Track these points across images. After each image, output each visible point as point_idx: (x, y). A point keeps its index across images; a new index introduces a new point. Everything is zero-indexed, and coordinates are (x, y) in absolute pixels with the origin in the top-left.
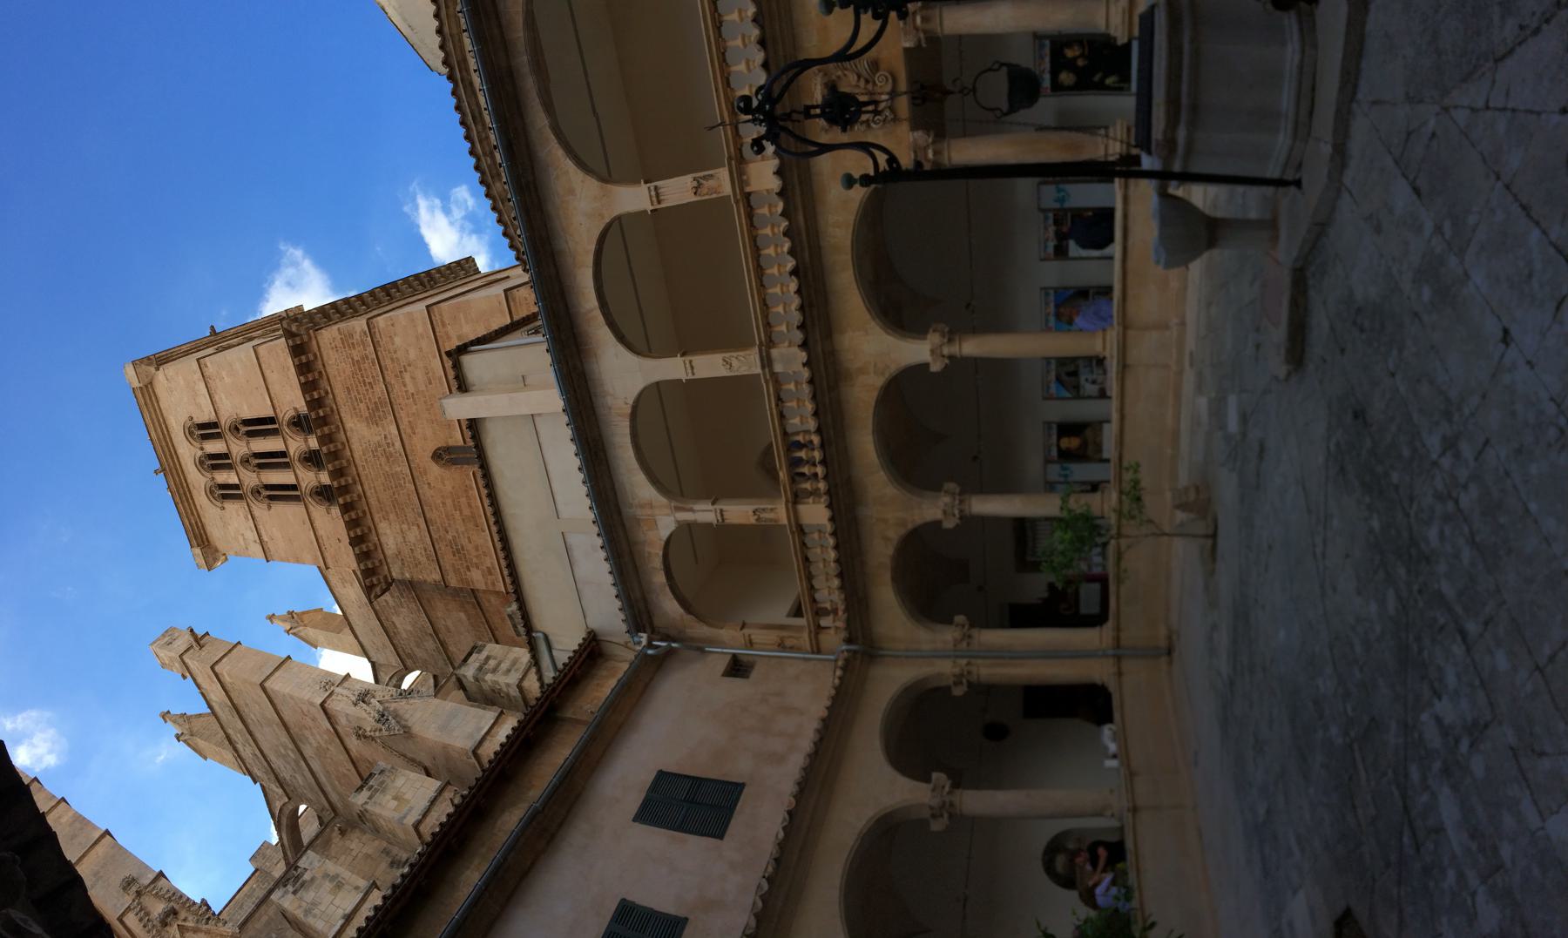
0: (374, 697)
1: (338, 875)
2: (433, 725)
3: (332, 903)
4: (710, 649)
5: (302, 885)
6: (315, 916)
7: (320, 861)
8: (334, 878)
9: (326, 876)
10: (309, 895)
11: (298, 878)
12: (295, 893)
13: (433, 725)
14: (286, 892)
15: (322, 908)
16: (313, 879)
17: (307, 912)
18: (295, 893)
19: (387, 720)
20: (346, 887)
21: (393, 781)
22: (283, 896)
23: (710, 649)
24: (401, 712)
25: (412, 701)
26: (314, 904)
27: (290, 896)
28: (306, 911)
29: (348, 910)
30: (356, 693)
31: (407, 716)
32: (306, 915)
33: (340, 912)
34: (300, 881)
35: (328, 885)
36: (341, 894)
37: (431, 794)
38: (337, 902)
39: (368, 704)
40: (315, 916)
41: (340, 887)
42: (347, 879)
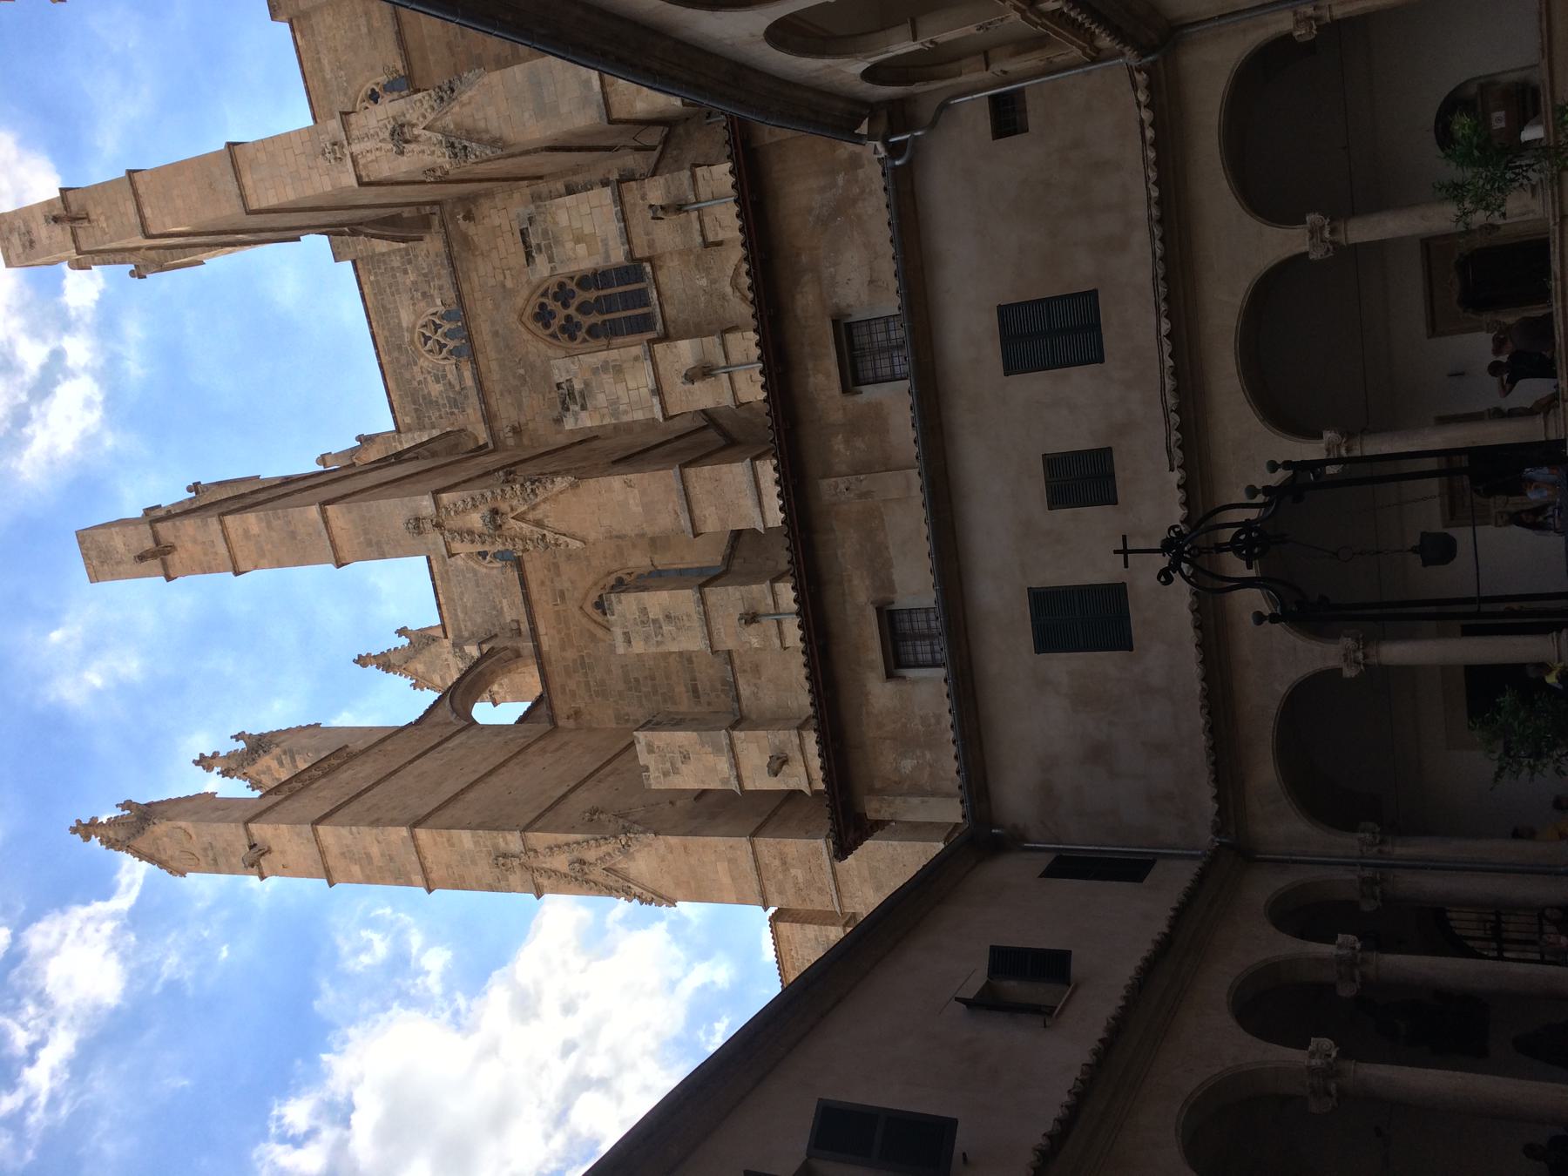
0: (413, 126)
1: (606, 362)
2: (527, 115)
3: (628, 390)
4: (956, 101)
5: (583, 396)
6: (626, 412)
7: (573, 363)
8: (605, 367)
9: (595, 371)
10: (601, 399)
11: (571, 393)
12: (584, 408)
13: (527, 115)
14: (575, 414)
15: (625, 400)
16: (587, 384)
17: (615, 414)
18: (584, 408)
19: (465, 148)
20: (625, 366)
21: (556, 223)
22: (577, 420)
23: (956, 101)
24: (468, 123)
25: (465, 98)
26: (614, 403)
27: (584, 414)
28: (612, 415)
29: (651, 383)
30: (387, 134)
31: (482, 124)
32: (617, 418)
33: (645, 392)
34: (576, 394)
35: (607, 379)
36: (628, 377)
37: (612, 210)
38: (632, 384)
39: (416, 139)
40: (626, 412)
41: (618, 370)
42: (618, 357)
